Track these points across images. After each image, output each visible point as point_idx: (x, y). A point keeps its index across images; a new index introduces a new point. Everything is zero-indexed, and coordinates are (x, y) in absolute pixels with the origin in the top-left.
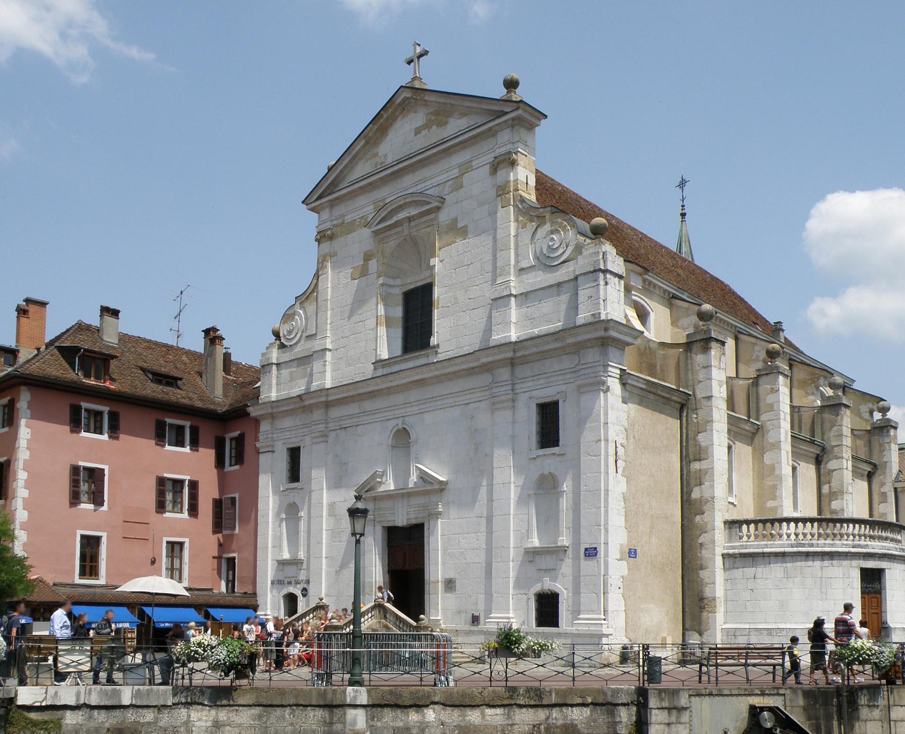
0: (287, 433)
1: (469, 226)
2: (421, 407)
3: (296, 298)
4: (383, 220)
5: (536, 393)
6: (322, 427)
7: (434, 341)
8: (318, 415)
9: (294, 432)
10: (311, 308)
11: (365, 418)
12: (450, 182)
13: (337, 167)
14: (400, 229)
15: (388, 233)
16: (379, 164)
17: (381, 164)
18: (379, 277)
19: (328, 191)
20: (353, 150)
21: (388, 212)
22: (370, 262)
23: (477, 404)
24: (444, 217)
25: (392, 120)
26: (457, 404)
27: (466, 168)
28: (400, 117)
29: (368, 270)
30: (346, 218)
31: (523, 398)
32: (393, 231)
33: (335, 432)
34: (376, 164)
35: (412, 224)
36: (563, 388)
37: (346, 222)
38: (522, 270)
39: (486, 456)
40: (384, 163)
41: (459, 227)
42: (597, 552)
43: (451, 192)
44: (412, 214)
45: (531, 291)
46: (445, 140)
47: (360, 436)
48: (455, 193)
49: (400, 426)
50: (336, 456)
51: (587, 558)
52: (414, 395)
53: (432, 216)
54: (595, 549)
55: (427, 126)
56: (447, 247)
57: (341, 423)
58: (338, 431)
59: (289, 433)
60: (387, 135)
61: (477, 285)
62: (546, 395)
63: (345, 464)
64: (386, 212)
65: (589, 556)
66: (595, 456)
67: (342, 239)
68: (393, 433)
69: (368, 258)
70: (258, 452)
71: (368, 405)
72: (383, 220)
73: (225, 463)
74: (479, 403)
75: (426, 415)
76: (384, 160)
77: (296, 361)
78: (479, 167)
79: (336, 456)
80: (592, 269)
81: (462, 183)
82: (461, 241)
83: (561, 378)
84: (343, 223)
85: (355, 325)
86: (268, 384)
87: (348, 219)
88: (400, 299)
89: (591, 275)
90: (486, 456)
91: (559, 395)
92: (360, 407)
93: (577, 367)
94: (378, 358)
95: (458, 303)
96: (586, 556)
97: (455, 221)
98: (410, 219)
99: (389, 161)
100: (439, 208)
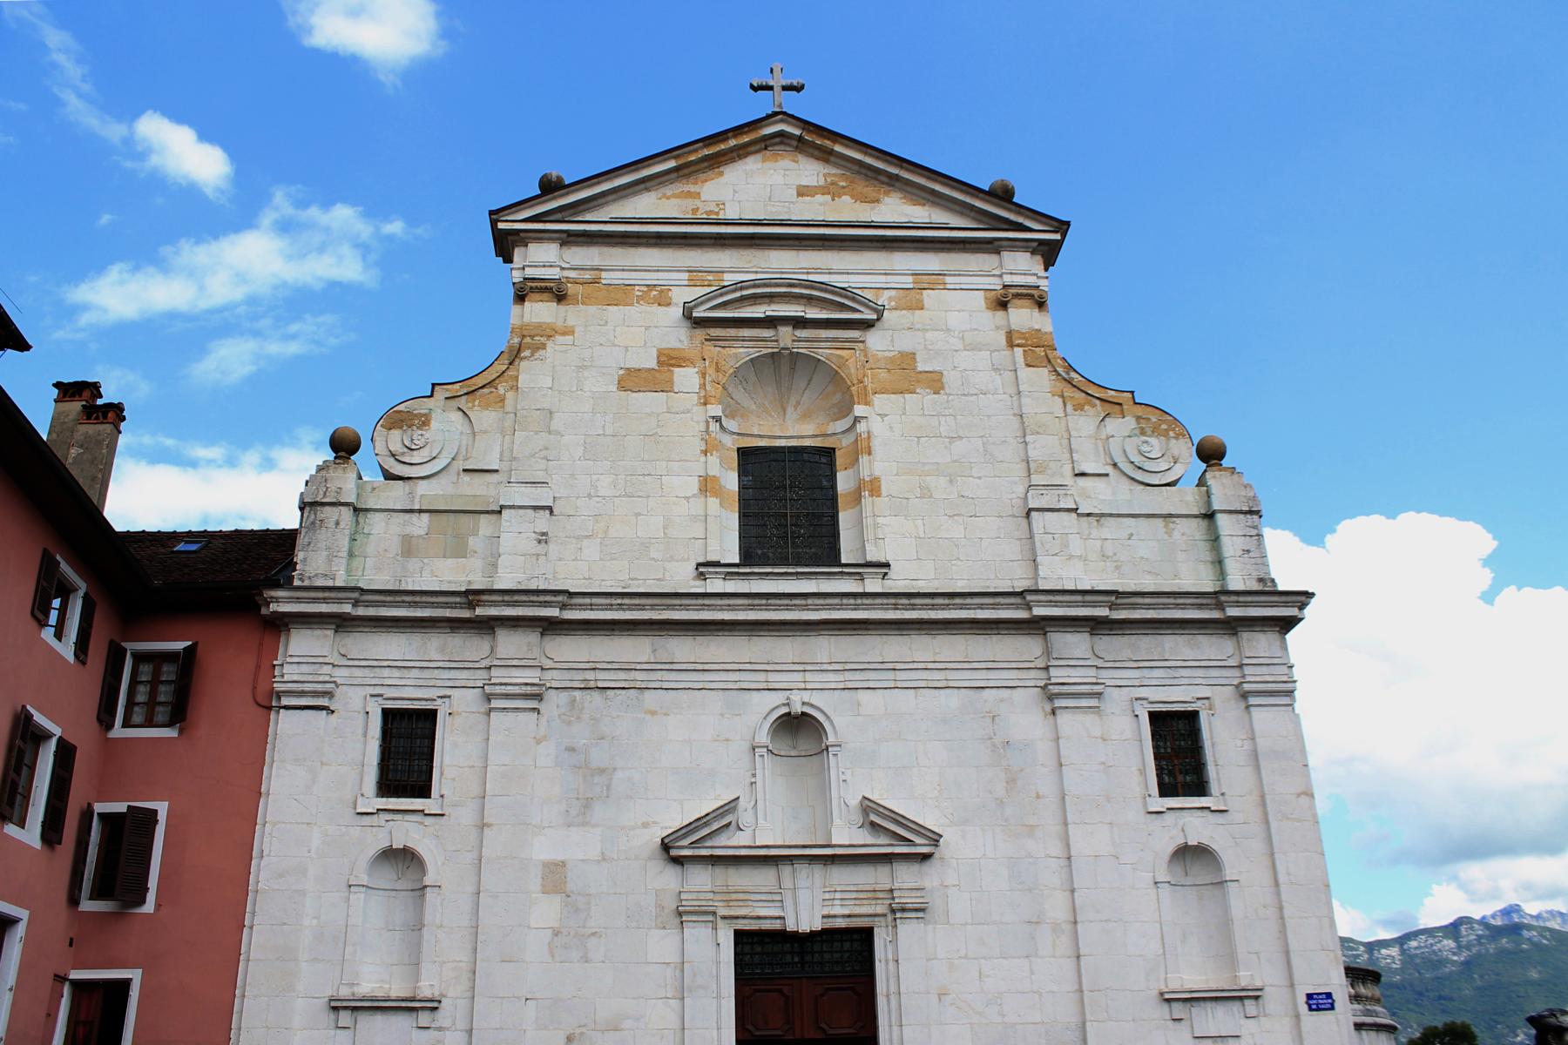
0: (386, 672)
1: (945, 373)
2: (848, 676)
3: (434, 385)
4: (724, 305)
5: (1143, 692)
6: (531, 676)
8: (510, 644)
9: (415, 673)
10: (485, 418)
11: (673, 676)
12: (893, 293)
13: (599, 183)
14: (767, 333)
15: (732, 332)
16: (700, 211)
17: (706, 213)
19: (558, 216)
20: (644, 167)
21: (742, 296)
22: (676, 370)
23: (1005, 693)
25: (741, 153)
26: (951, 684)
27: (933, 281)
28: (759, 156)
29: (671, 382)
30: (604, 275)
31: (1116, 700)
32: (746, 332)
33: (564, 695)
36: (1205, 692)
37: (604, 282)
38: (1083, 474)
39: (1038, 797)
40: (717, 213)
41: (919, 369)
42: (1334, 1001)
43: (896, 309)
44: (808, 316)
45: (1111, 515)
46: (873, 224)
47: (653, 713)
48: (904, 312)
50: (571, 749)
51: (1314, 1013)
52: (825, 648)
54: (1329, 995)
55: (830, 190)
56: (892, 395)
57: (590, 675)
58: (577, 694)
59: (396, 673)
60: (721, 174)
61: (980, 478)
62: (1176, 696)
63: (602, 771)
64: (738, 294)
65: (1318, 1009)
66: (1299, 821)
67: (592, 309)
69: (672, 362)
70: (268, 703)
71: (682, 648)
72: (724, 305)
73: (115, 716)
74: (1009, 691)
75: (863, 696)
76: (717, 210)
77: (425, 516)
78: (961, 289)
79: (571, 749)
80: (1245, 508)
81: (922, 301)
82: (928, 394)
83: (1200, 672)
84: (595, 281)
85: (629, 478)
86: (328, 548)
89: (1242, 516)
90: (1038, 797)
91: (1199, 703)
92: (654, 651)
93: (1230, 660)
94: (712, 558)
95: (931, 497)
96: (1311, 1009)
98: (799, 323)
99: (731, 213)
100: (867, 325)
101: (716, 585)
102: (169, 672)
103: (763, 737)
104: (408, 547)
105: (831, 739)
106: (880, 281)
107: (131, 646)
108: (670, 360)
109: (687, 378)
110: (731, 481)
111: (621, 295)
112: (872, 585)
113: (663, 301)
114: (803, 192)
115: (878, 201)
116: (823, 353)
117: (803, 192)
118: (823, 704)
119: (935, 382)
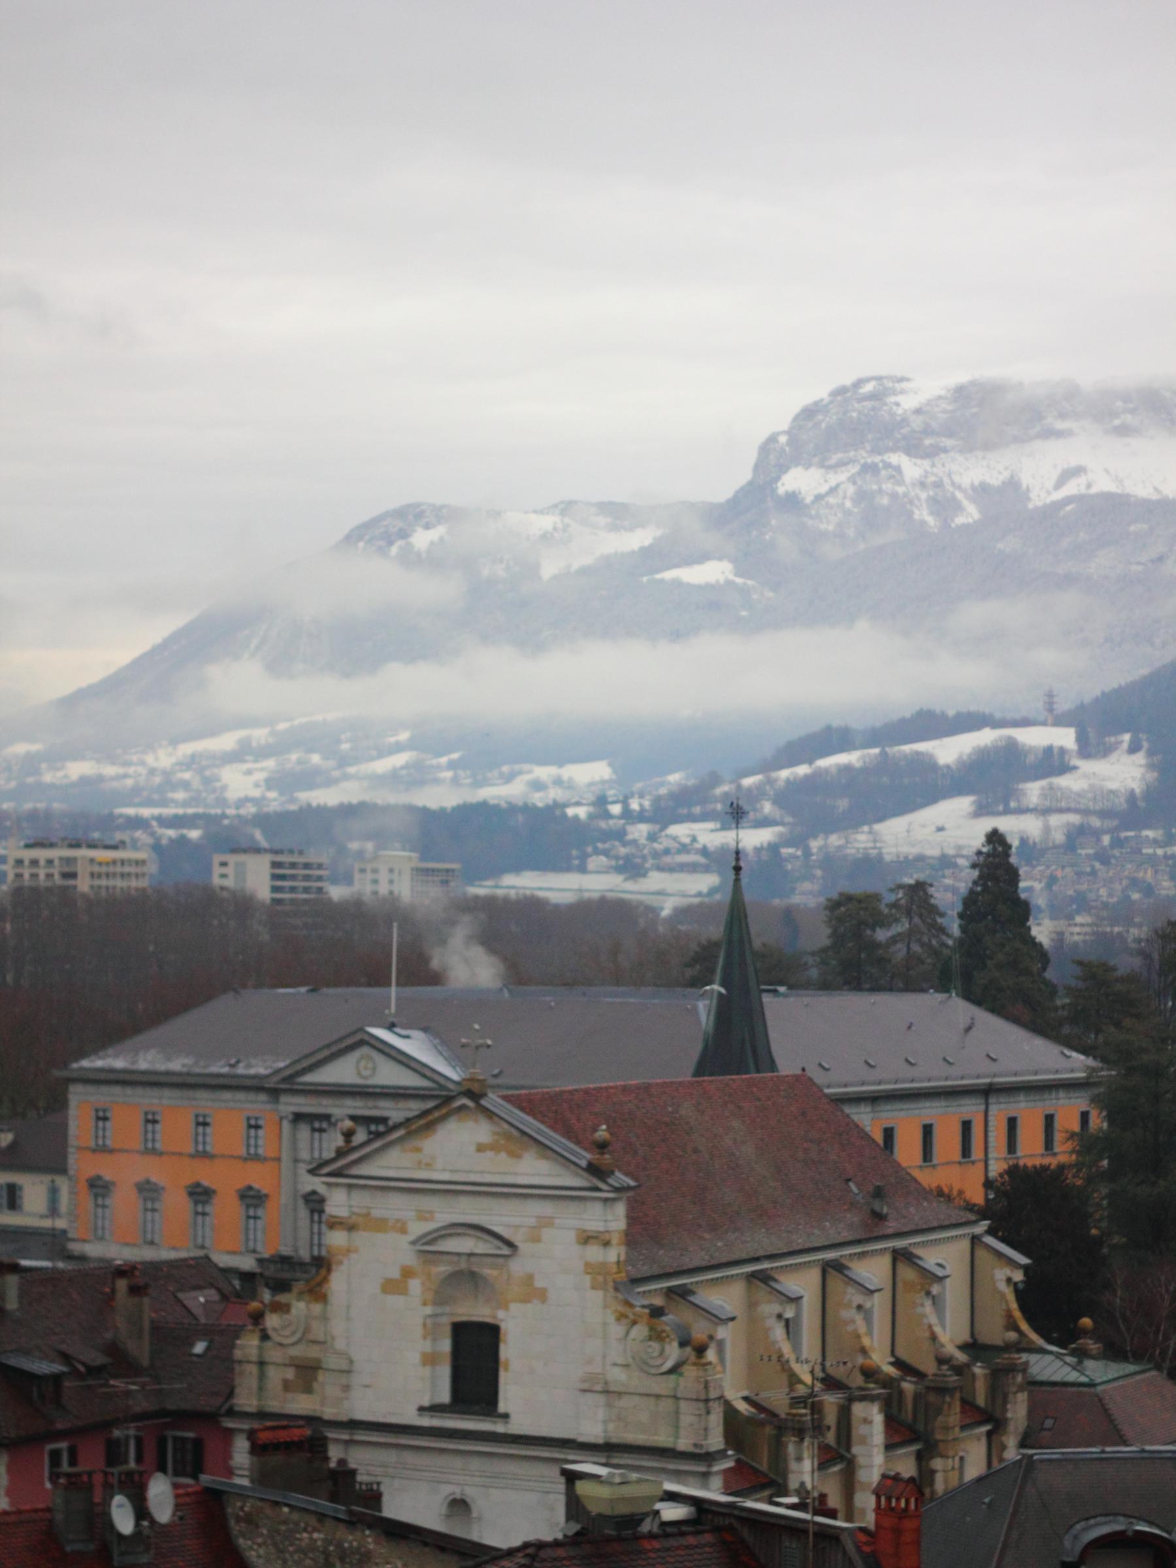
7: (502, 1407)
14: (455, 1259)
17: (428, 1165)
18: (425, 1304)
24: (517, 1267)
34: (420, 1163)
35: (473, 1259)
49: (458, 1496)
52: (475, 1464)
53: (501, 1260)
55: (493, 1147)
57: (369, 1468)
68: (448, 1500)
71: (410, 1458)
75: (492, 1491)
87: (376, 1213)
88: (447, 1331)
97: (530, 1278)
101: (426, 1421)
102: (189, 1446)
103: (444, 1510)
104: (287, 1386)
105: (475, 1515)
106: (516, 1221)
107: (170, 1434)
108: (407, 1273)
109: (415, 1285)
110: (446, 1345)
111: (380, 1225)
112: (500, 1428)
113: (403, 1230)
114: (481, 1148)
115: (519, 1157)
116: (487, 1272)
117: (481, 1148)
118: (471, 1493)
119: (541, 1295)
